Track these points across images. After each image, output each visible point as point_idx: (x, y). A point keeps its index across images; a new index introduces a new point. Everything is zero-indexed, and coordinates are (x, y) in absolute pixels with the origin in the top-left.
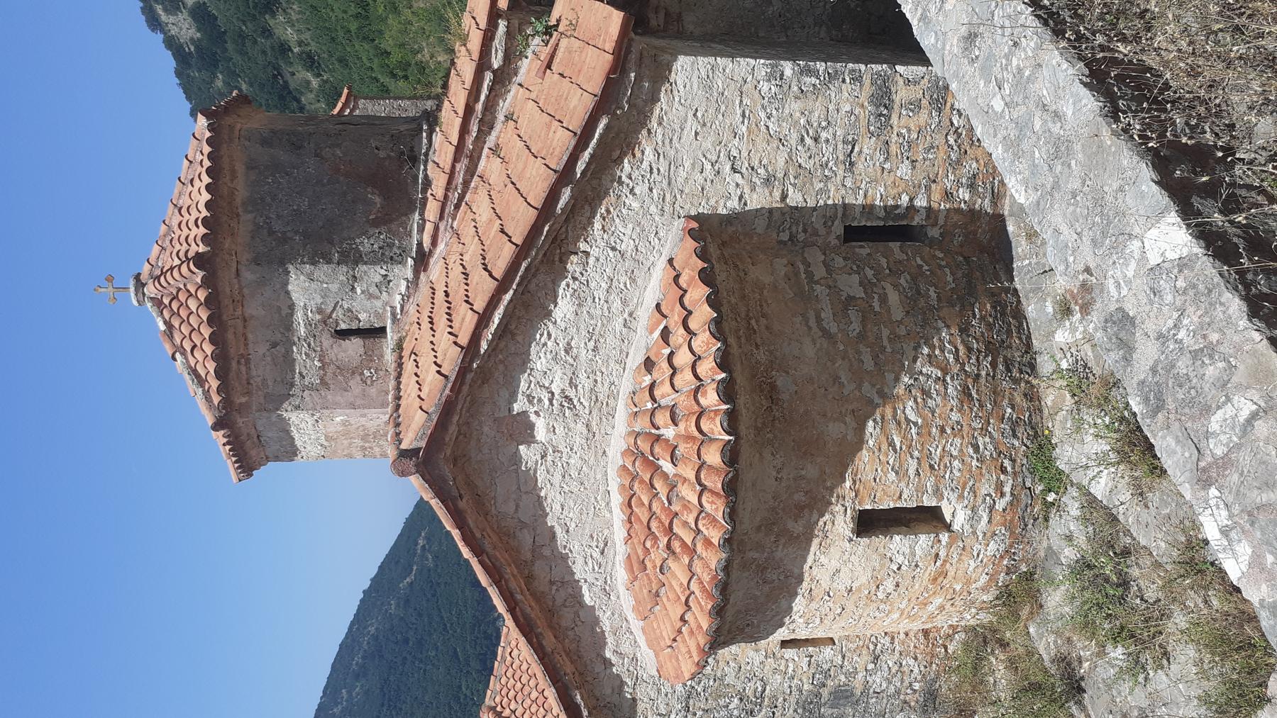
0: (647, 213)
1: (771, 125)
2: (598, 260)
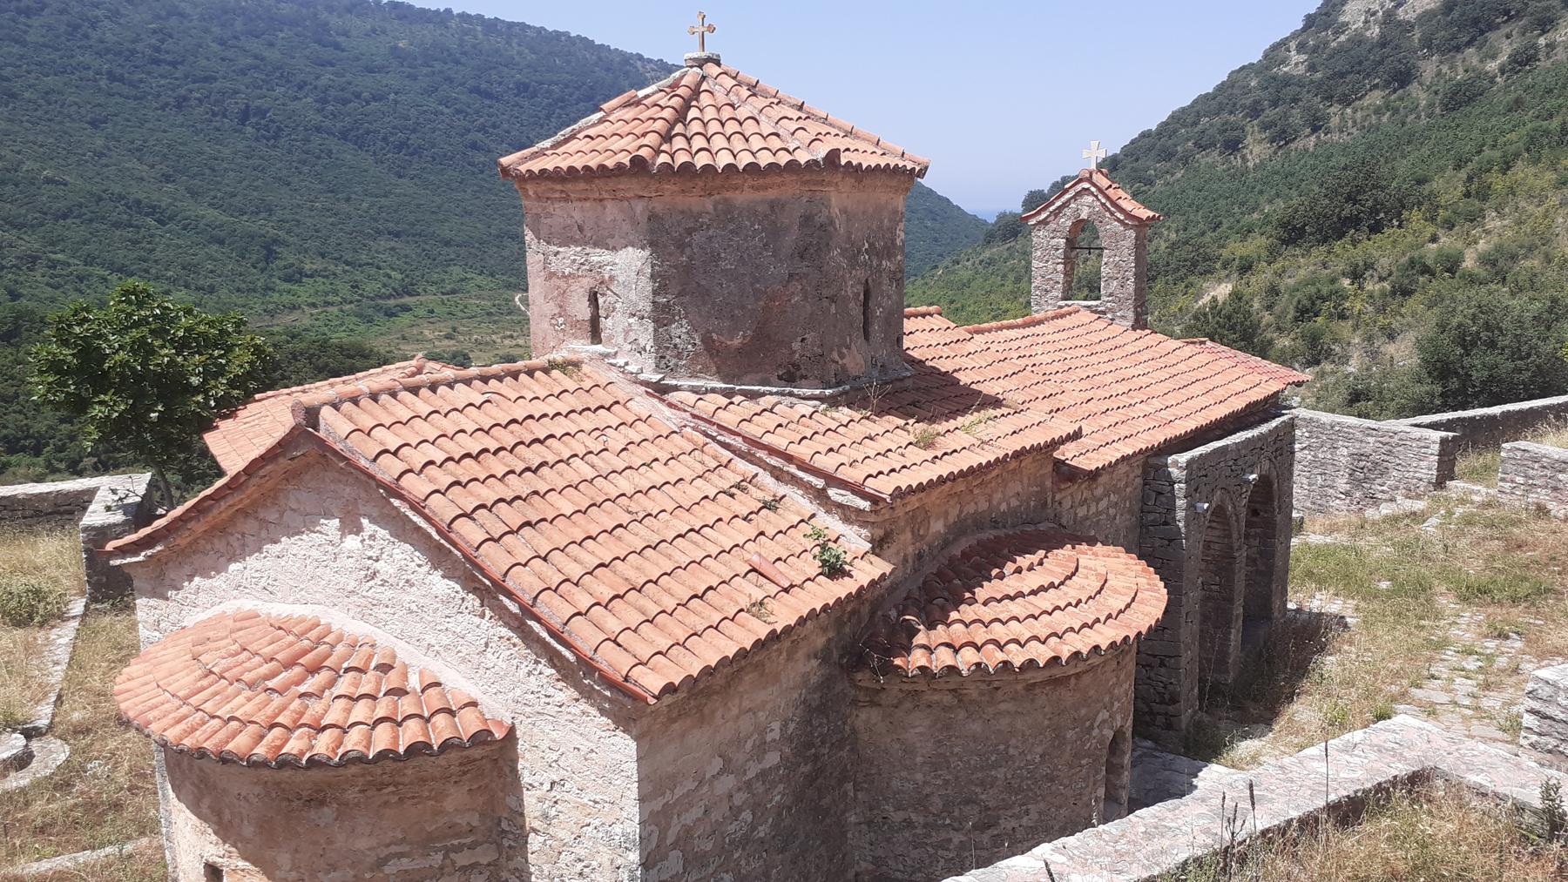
1: (590, 829)
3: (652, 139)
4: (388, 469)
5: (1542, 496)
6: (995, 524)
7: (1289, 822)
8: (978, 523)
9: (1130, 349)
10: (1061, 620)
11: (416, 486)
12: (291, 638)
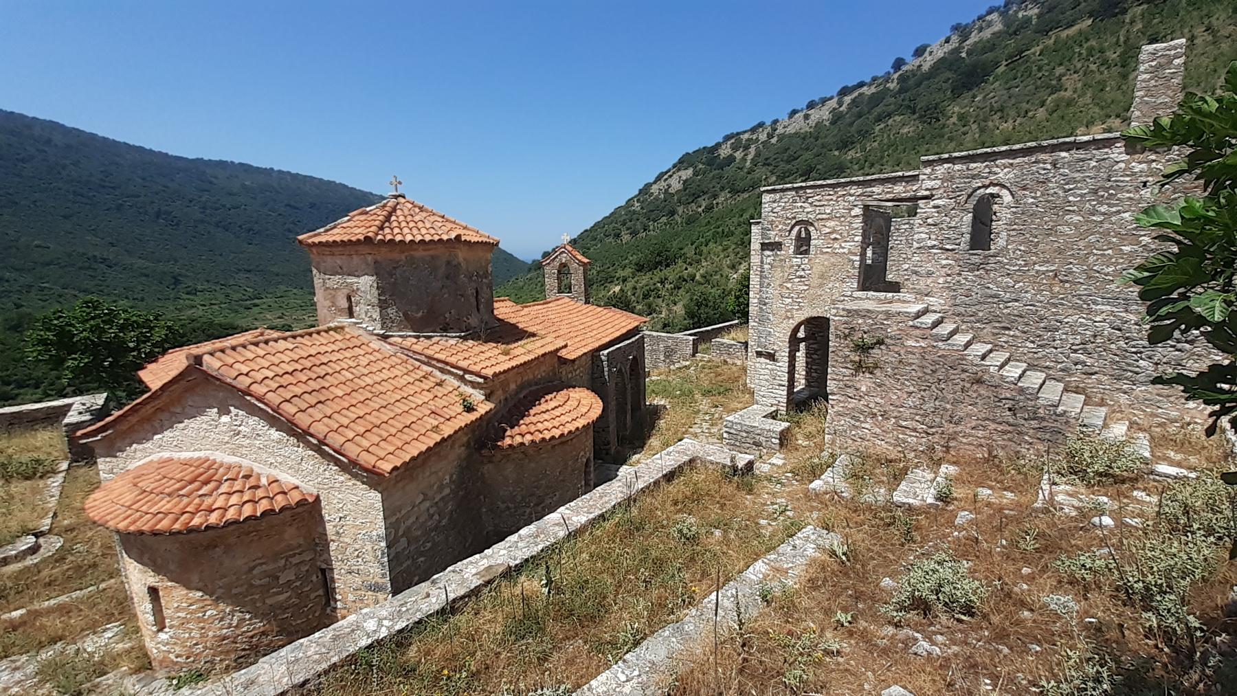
0: (318, 476)
2: (297, 452)
3: (374, 229)
4: (243, 382)
5: (725, 357)
6: (536, 384)
7: (650, 484)
8: (530, 384)
9: (584, 312)
10: (564, 419)
11: (259, 389)
12: (193, 469)
